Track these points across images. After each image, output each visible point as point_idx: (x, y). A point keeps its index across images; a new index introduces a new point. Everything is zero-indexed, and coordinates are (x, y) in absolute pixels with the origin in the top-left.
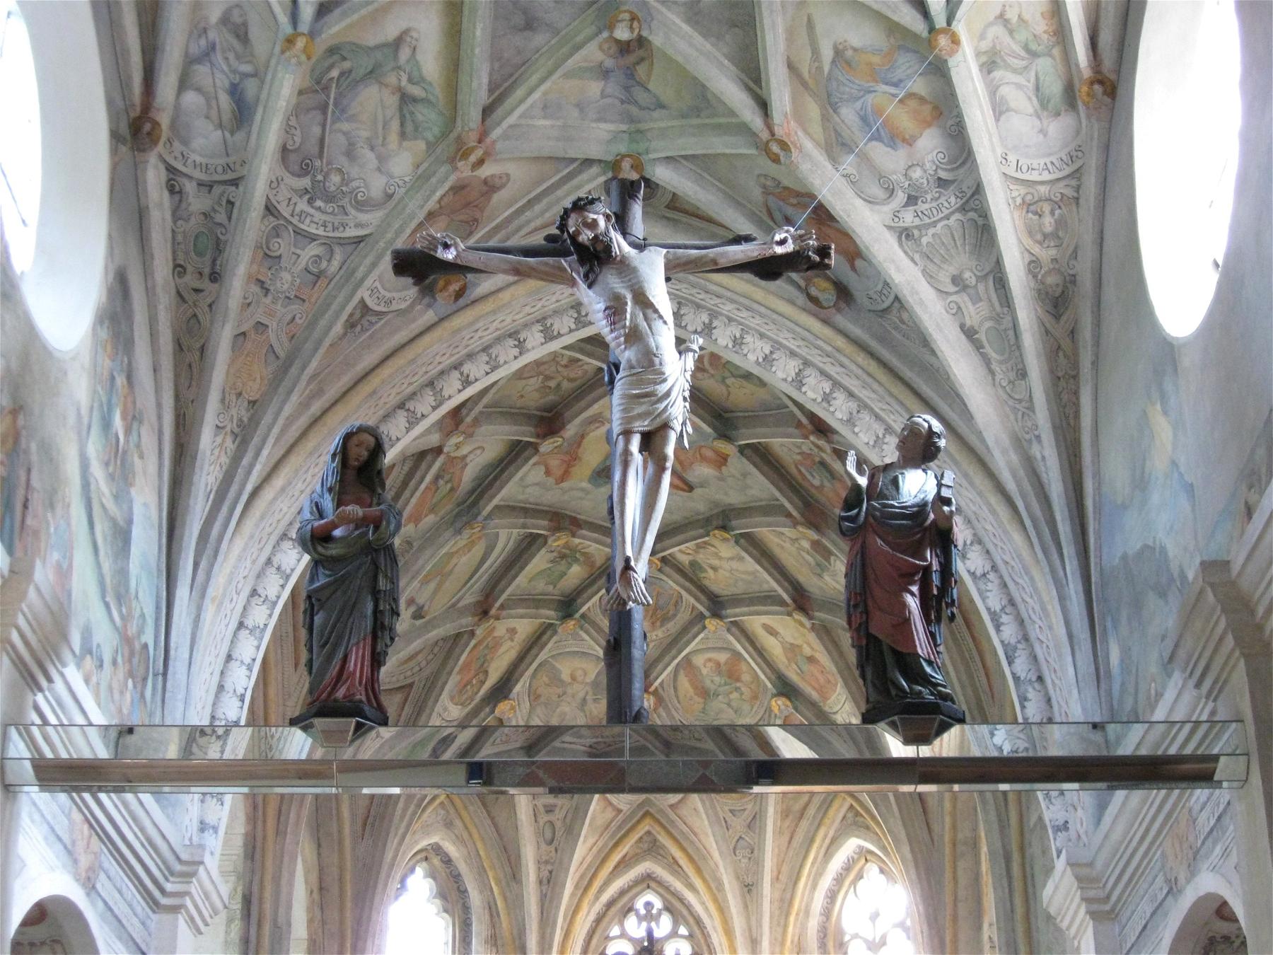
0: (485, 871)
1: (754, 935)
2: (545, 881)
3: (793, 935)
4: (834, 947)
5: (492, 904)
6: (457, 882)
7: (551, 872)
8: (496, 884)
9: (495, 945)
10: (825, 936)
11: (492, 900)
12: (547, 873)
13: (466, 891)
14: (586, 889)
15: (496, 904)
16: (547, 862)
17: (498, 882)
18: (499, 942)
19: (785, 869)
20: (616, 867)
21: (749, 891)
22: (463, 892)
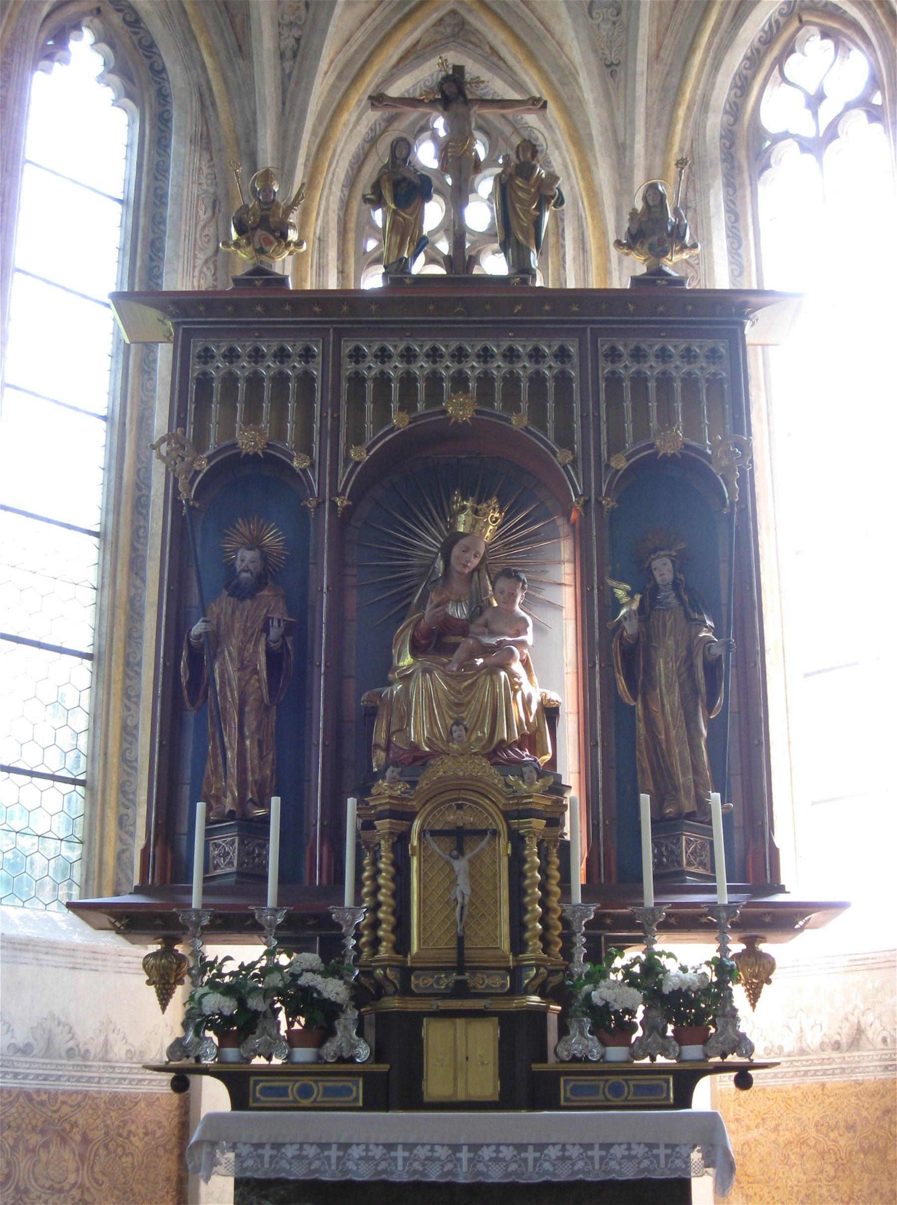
0: (194, 38)
1: (621, 138)
2: (289, 54)
3: (682, 141)
4: (748, 157)
5: (204, 88)
6: (149, 57)
7: (298, 40)
8: (211, 55)
9: (209, 149)
10: (732, 145)
11: (204, 84)
12: (291, 42)
13: (164, 70)
14: (355, 80)
15: (210, 89)
16: (291, 25)
17: (214, 54)
18: (215, 146)
19: (668, 41)
20: (402, 59)
21: (613, 74)
22: (158, 72)
